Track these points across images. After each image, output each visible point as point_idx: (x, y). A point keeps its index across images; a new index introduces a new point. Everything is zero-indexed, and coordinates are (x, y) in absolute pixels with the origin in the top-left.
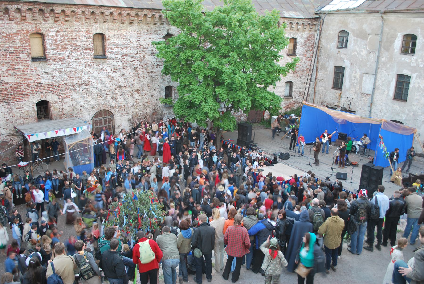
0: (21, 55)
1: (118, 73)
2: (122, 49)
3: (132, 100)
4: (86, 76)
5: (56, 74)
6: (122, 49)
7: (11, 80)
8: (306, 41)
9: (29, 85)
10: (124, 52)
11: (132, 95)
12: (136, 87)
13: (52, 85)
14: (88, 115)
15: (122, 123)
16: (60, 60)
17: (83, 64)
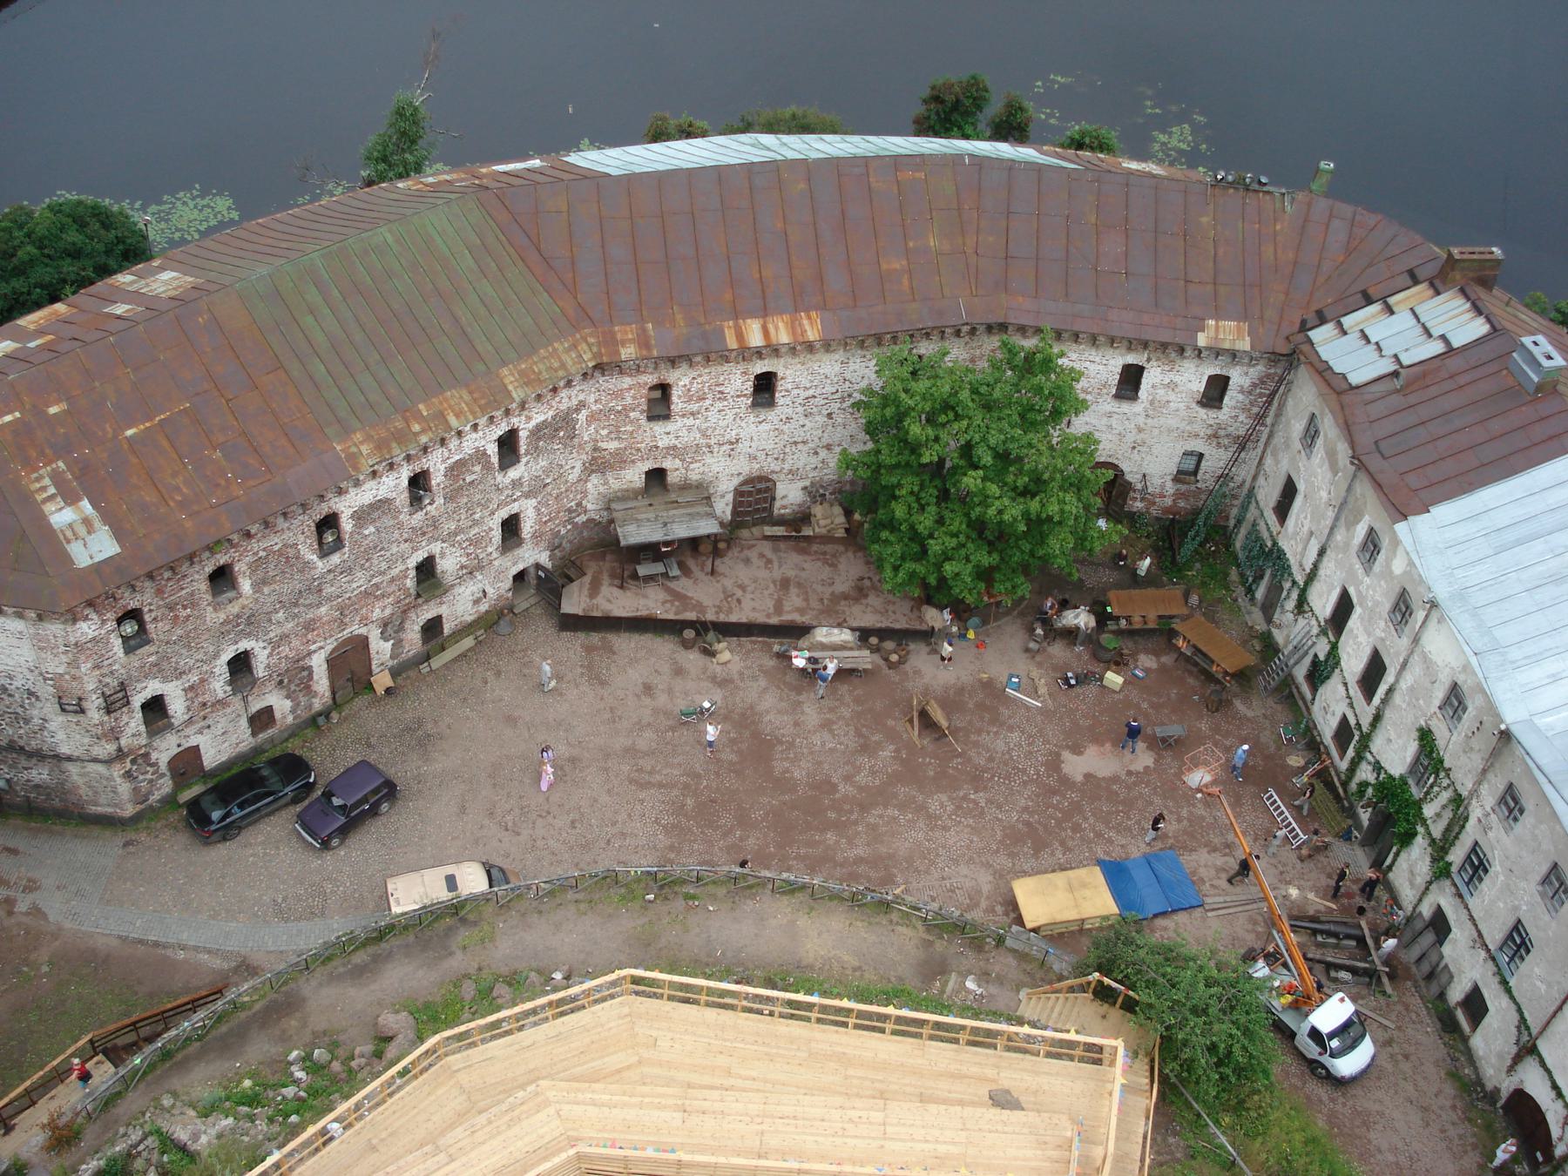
1: (793, 425)
2: (806, 389)
3: (814, 461)
6: (806, 389)
7: (613, 446)
8: (1254, 385)
9: (639, 450)
10: (811, 392)
11: (816, 453)
12: (825, 441)
13: (674, 448)
16: (692, 414)
17: (730, 417)
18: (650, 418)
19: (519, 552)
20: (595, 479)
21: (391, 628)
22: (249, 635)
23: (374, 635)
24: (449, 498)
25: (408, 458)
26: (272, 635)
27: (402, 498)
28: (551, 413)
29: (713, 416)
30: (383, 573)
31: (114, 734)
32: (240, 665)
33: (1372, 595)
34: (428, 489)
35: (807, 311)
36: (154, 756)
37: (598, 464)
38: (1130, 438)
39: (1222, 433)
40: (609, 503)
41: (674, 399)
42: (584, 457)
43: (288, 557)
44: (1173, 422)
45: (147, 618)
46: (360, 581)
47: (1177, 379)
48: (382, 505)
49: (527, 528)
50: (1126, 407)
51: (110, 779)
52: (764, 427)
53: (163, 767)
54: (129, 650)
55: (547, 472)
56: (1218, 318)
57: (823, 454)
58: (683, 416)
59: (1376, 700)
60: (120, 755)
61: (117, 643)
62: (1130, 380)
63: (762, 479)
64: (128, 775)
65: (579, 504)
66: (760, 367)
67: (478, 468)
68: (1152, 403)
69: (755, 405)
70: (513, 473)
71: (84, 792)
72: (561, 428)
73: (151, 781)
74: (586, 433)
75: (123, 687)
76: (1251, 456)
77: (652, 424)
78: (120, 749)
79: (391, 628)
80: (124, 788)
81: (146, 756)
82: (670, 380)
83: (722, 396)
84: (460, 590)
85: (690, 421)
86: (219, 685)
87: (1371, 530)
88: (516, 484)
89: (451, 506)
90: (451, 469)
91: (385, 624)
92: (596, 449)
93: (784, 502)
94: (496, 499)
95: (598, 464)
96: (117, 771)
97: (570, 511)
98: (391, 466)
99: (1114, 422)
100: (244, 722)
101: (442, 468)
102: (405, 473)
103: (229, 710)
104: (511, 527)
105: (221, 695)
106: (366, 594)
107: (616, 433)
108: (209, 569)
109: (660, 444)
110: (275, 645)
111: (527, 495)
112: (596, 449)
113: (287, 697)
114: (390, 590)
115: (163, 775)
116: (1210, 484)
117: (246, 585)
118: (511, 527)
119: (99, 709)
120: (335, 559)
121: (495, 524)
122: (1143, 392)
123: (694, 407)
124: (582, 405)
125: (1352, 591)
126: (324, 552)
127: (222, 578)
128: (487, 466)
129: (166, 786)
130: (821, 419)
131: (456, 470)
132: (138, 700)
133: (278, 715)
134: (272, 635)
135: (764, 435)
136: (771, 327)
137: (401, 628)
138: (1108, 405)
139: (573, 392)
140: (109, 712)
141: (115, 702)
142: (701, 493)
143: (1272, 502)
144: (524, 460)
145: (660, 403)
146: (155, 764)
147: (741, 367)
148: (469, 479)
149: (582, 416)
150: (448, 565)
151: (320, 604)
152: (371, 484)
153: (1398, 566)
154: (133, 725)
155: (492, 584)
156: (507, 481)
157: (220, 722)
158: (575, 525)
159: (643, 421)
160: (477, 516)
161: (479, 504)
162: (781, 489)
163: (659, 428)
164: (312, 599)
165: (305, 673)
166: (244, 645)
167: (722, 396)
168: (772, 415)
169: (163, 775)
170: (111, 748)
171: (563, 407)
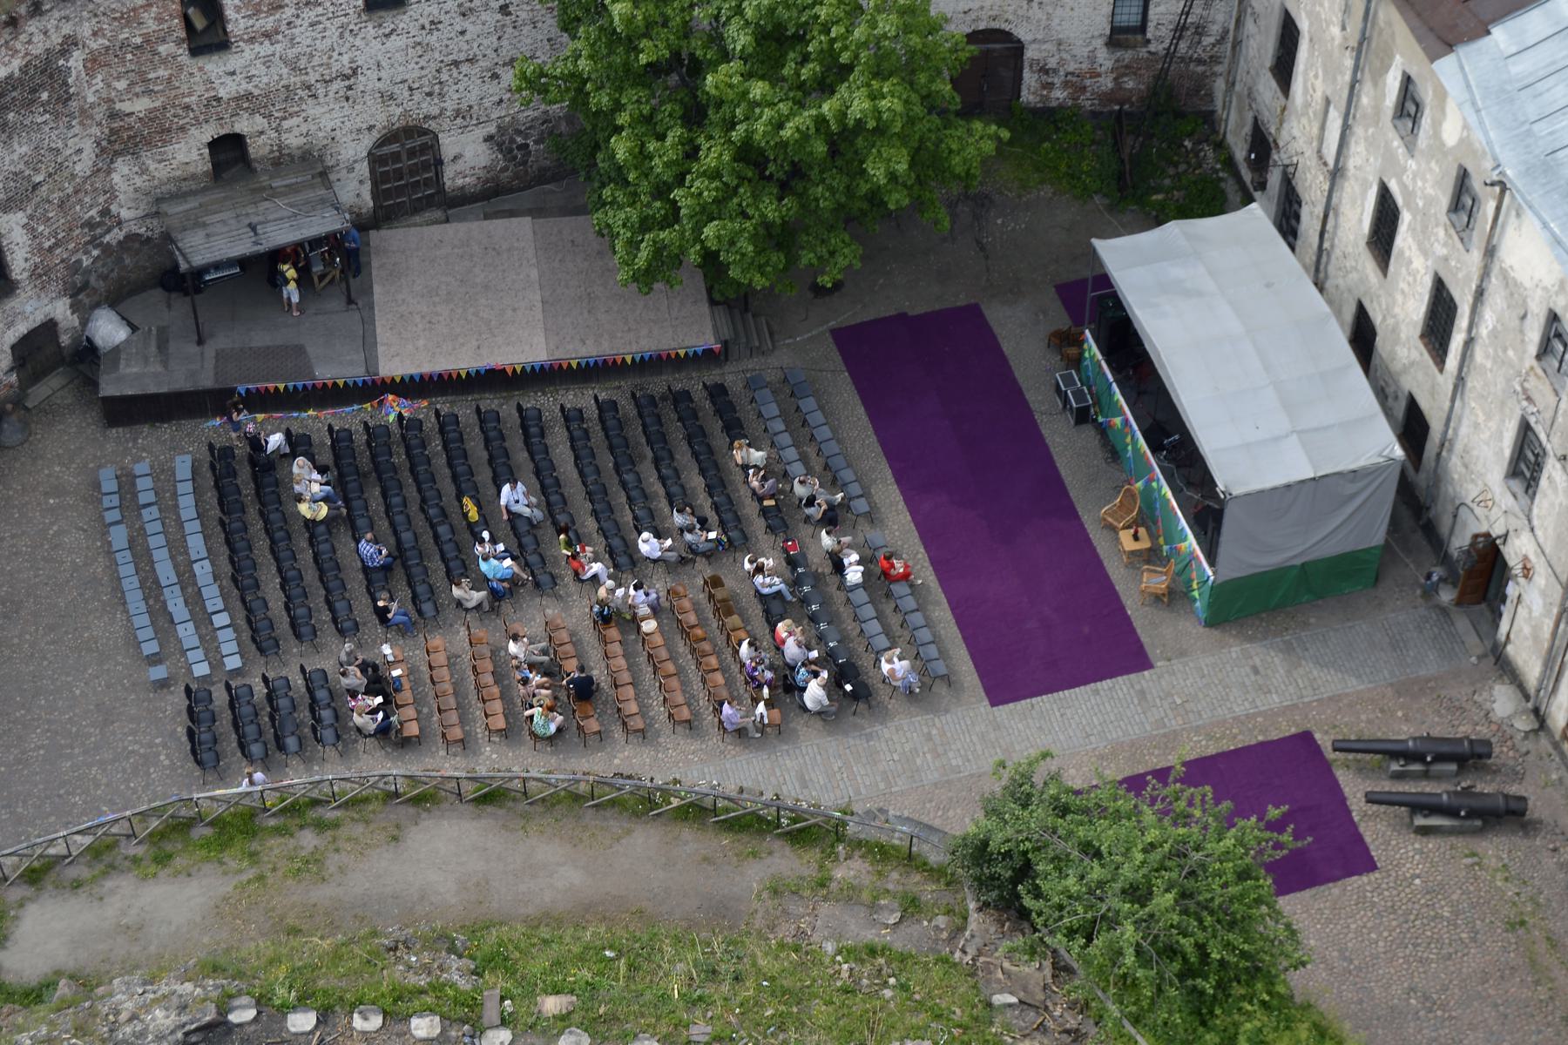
0: (162, 49)
1: (446, 31)
3: (494, 90)
4: (345, 59)
5: (258, 69)
7: (141, 106)
9: (187, 107)
11: (495, 76)
12: (506, 53)
13: (248, 96)
14: (353, 151)
15: (467, 155)
16: (267, 35)
17: (333, 32)
18: (195, 52)
28: (16, 64)
29: (303, 34)
33: (1423, 190)
40: (158, 201)
42: (95, 131)
52: (396, 42)
55: (33, 163)
58: (252, 40)
59: (1452, 361)
65: (105, 212)
74: (91, 91)
77: (201, 61)
85: (265, 48)
87: (1407, 81)
92: (113, 115)
93: (460, 166)
95: (122, 140)
97: (90, 224)
109: (222, 93)
123: (268, 23)
124: (70, 43)
125: (1393, 186)
130: (491, 18)
135: (399, 57)
139: (50, 22)
142: (312, 166)
149: (76, 61)
153: (1451, 133)
158: (107, 249)
162: (449, 144)
163: (213, 66)
171: (38, 49)
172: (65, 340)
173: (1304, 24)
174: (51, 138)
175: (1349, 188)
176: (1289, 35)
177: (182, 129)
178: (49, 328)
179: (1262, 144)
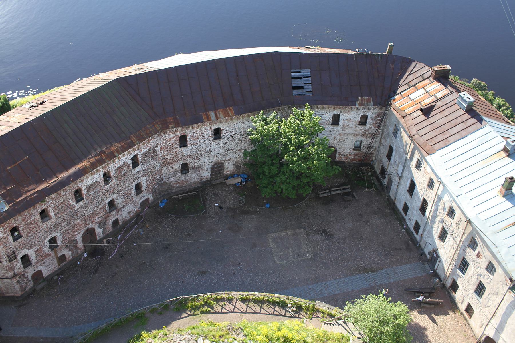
0: (175, 146)
1: (228, 144)
2: (231, 132)
3: (236, 155)
5: (192, 150)
6: (231, 132)
7: (169, 157)
8: (376, 117)
9: (178, 157)
10: (233, 133)
12: (239, 149)
14: (208, 167)
15: (229, 168)
16: (195, 144)
17: (207, 144)
19: (141, 195)
20: (164, 168)
21: (102, 224)
22: (55, 231)
23: (96, 227)
24: (117, 179)
25: (103, 168)
26: (63, 230)
27: (102, 181)
28: (148, 148)
29: (201, 144)
30: (97, 206)
31: (12, 269)
32: (53, 241)
34: (110, 177)
35: (229, 107)
36: (26, 275)
37: (165, 163)
38: (338, 137)
39: (367, 133)
41: (188, 140)
42: (160, 161)
43: (66, 205)
44: (351, 131)
45: (20, 229)
46: (90, 210)
47: (351, 117)
48: (95, 184)
49: (144, 187)
50: (335, 128)
51: (12, 284)
52: (219, 146)
53: (30, 278)
54: (15, 240)
56: (362, 97)
57: (239, 153)
58: (192, 145)
60: (15, 276)
61: (11, 238)
62: (336, 120)
63: (219, 163)
64: (18, 282)
66: (215, 127)
67: (126, 169)
68: (344, 126)
69: (215, 139)
70: (138, 169)
71: (4, 289)
72: (152, 153)
73: (26, 283)
74: (160, 154)
75: (14, 253)
76: (377, 140)
77: (182, 148)
78: (15, 274)
79: (102, 224)
80: (17, 286)
81: (24, 275)
82: (186, 134)
83: (204, 137)
84: (123, 209)
85: (194, 147)
86: (46, 249)
88: (139, 173)
89: (118, 182)
90: (117, 170)
91: (100, 223)
92: (164, 159)
93: (228, 170)
94: (132, 178)
96: (14, 281)
97: (157, 180)
98: (97, 171)
99: (332, 133)
100: (55, 260)
101: (114, 170)
102: (102, 173)
103: (50, 257)
104: (138, 187)
105: (47, 252)
106: (93, 214)
107: (170, 153)
108: (40, 211)
110: (64, 234)
111: (142, 176)
112: (164, 159)
113: (70, 250)
114: (100, 212)
115: (30, 281)
116: (365, 150)
117: (52, 214)
118: (138, 187)
119: (6, 261)
120: (81, 203)
121: (133, 186)
122: (340, 123)
123: (195, 142)
124: (158, 145)
126: (77, 202)
127: (44, 214)
128: (129, 168)
129: (31, 284)
130: (237, 142)
131: (119, 170)
132: (19, 257)
133: (67, 257)
134: (63, 230)
135: (219, 149)
136: (218, 113)
137: (105, 224)
138: (330, 128)
140: (10, 262)
141: (12, 257)
143: (386, 154)
144: (141, 165)
145: (183, 141)
146: (27, 277)
147: (209, 127)
148: (123, 173)
149: (159, 148)
150: (119, 201)
151: (77, 219)
152: (91, 177)
154: (18, 265)
155: (134, 206)
156: (136, 172)
157: (48, 261)
159: (179, 148)
160: (127, 185)
161: (127, 180)
162: (226, 166)
163: (184, 149)
164: (75, 217)
165: (75, 242)
166: (54, 235)
167: (204, 137)
168: (220, 142)
169: (30, 281)
170: (11, 274)
171: (152, 146)
172: (150, 202)
173: (394, 148)
174: (152, 163)
175: (402, 182)
176: (391, 150)
177: (176, 162)
178: (148, 199)
179: (383, 171)
